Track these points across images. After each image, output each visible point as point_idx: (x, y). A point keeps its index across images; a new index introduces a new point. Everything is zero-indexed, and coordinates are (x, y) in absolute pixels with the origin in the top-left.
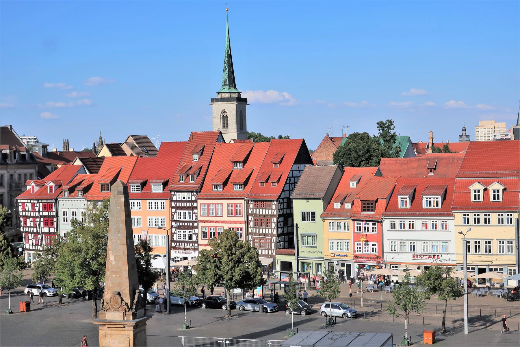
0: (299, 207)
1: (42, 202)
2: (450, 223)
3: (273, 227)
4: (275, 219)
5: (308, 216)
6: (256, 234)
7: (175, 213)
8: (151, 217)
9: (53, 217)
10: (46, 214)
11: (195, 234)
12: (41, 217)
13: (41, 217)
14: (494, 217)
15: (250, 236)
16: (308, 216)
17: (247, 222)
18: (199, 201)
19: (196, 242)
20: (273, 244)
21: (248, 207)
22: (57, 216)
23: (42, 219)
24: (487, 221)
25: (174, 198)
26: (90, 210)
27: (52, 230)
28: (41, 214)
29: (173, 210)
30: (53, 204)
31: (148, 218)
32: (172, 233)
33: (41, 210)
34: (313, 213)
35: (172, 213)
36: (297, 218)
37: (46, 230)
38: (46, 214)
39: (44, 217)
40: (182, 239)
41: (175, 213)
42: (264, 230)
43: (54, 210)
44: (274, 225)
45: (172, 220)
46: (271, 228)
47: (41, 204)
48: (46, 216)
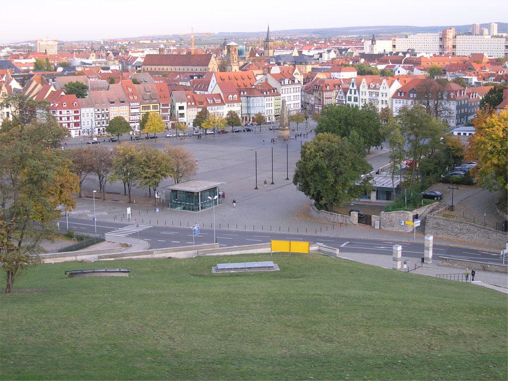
0: (178, 105)
2: (224, 107)
4: (169, 110)
5: (181, 108)
14: (235, 104)
16: (181, 108)
17: (159, 111)
18: (141, 106)
21: (160, 106)
22: (80, 115)
24: (234, 106)
25: (131, 105)
27: (78, 121)
34: (183, 107)
36: (177, 108)
38: (75, 114)
44: (169, 112)
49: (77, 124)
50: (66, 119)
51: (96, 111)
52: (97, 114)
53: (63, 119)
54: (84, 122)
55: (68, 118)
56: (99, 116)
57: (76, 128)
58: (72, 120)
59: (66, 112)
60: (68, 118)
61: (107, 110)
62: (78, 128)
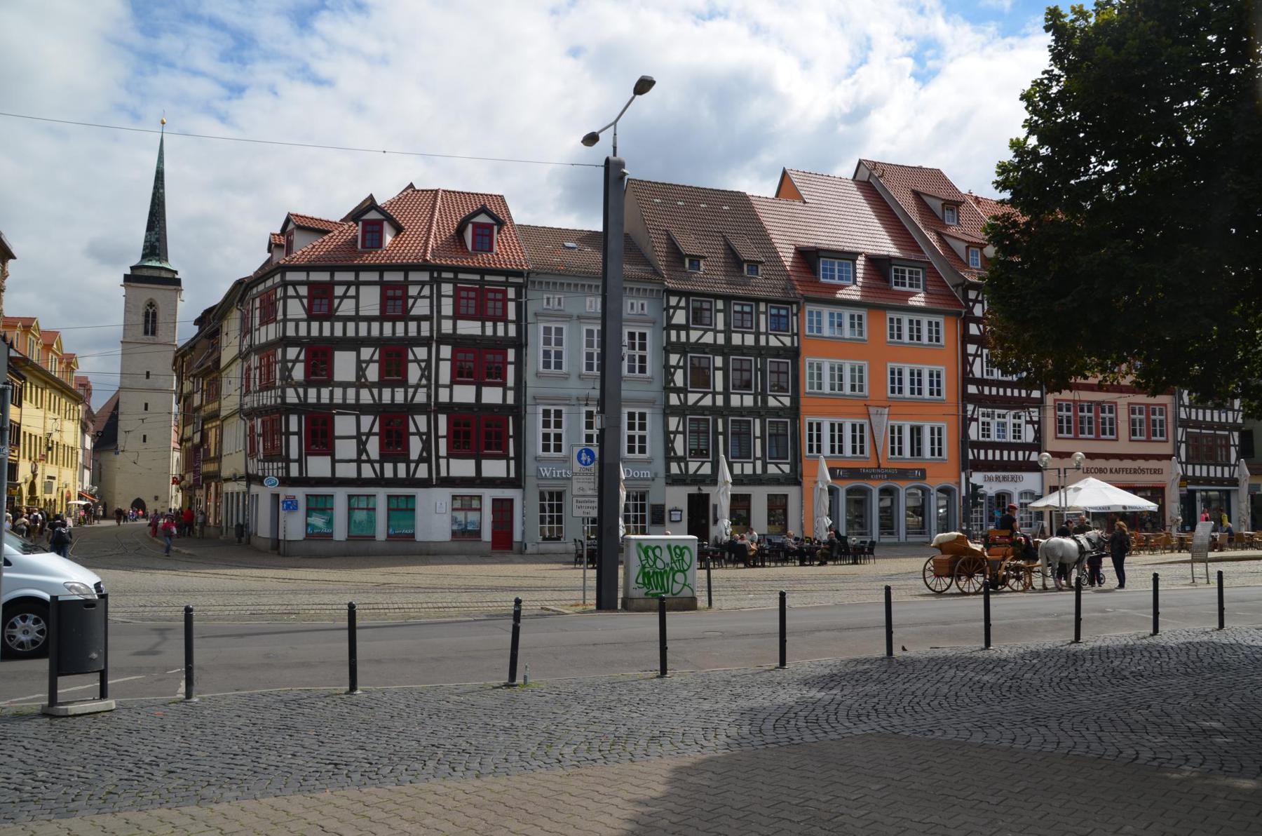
1: (454, 281)
3: (1236, 407)
6: (1197, 424)
7: (975, 355)
8: (896, 365)
9: (506, 343)
10: (469, 328)
11: (1031, 422)
12: (443, 339)
13: (443, 339)
15: (1180, 430)
19: (1037, 446)
20: (1233, 449)
22: (520, 343)
23: (446, 351)
26: (678, 328)
27: (492, 395)
28: (447, 327)
29: (971, 349)
30: (511, 293)
31: (890, 365)
32: (965, 417)
33: (447, 307)
35: (965, 355)
37: (464, 394)
38: (469, 328)
39: (455, 341)
40: (994, 437)
41: (975, 355)
42: (1208, 412)
43: (512, 315)
45: (967, 378)
46: (1234, 410)
47: (447, 289)
48: (472, 338)
49: (479, 432)
50: (373, 373)
51: (680, 318)
52: (683, 349)
53: (344, 365)
54: (553, 418)
55: (393, 358)
56: (700, 378)
57: (463, 468)
58: (439, 382)
59: (370, 300)
60: (393, 358)
61: (779, 325)
62: (494, 468)
